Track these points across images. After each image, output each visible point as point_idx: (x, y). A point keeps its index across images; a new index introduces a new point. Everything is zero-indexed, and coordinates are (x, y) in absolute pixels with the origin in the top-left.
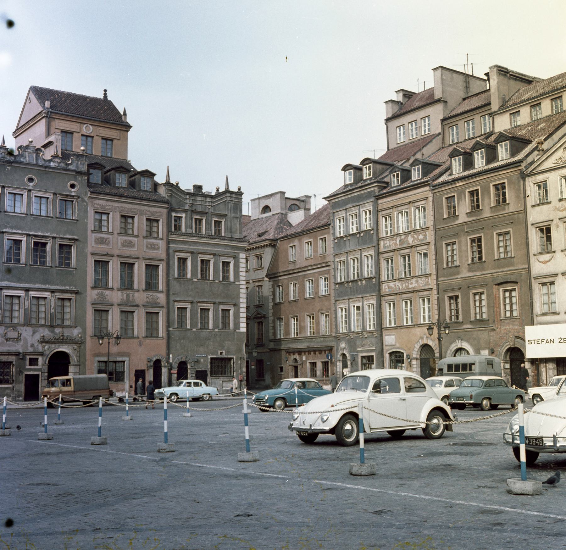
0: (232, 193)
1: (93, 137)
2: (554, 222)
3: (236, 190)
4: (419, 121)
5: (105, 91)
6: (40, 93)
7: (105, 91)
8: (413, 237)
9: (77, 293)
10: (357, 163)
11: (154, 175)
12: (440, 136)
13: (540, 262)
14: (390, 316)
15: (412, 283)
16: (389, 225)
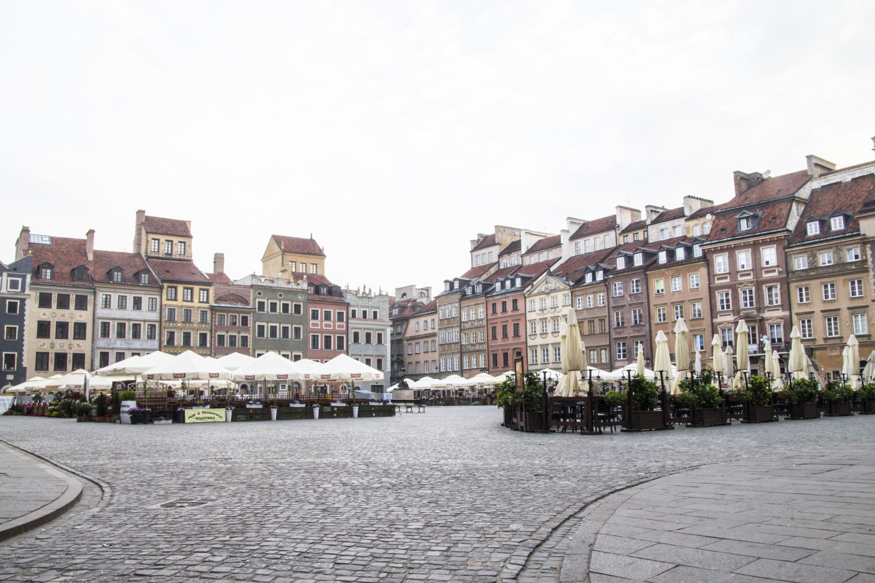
6: (277, 239)
10: (451, 279)
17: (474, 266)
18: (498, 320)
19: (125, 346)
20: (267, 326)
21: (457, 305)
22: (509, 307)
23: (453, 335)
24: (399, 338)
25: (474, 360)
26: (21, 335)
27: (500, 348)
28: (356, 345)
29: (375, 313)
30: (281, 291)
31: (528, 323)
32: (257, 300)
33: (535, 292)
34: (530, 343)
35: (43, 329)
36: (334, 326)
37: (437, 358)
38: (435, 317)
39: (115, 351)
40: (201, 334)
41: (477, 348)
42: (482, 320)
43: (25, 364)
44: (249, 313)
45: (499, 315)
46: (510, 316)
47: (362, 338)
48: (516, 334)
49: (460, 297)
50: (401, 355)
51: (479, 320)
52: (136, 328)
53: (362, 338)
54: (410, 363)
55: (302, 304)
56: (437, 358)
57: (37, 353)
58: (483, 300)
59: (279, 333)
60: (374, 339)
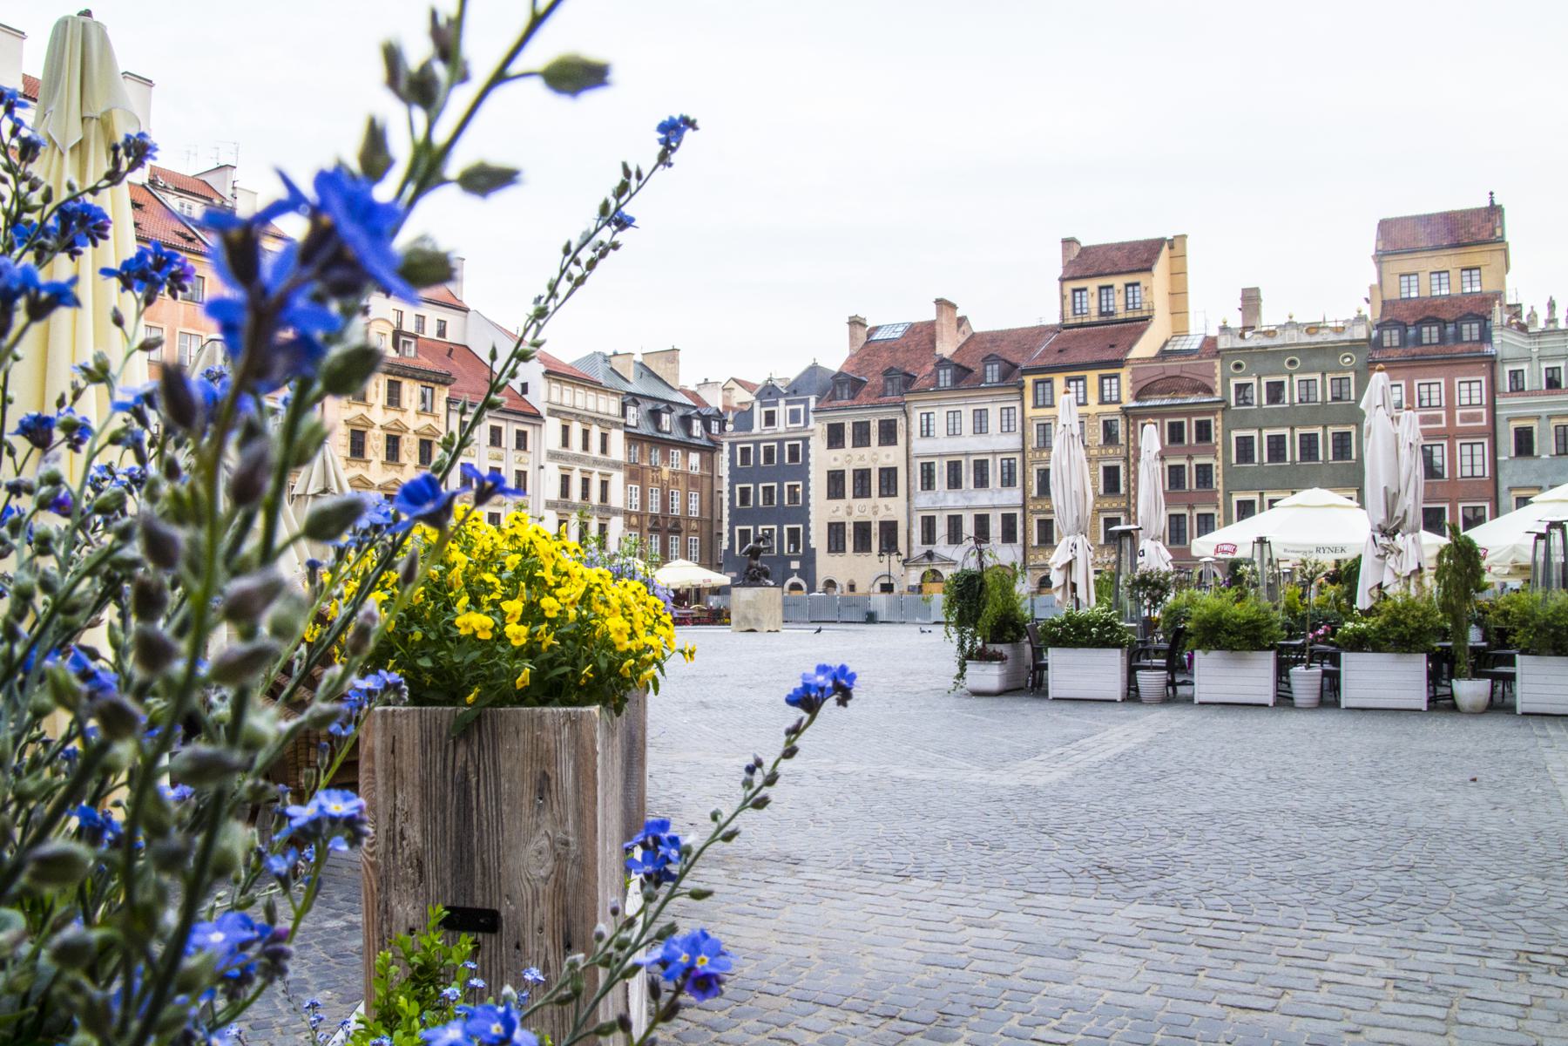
6: (1385, 226)
19: (962, 503)
20: (1260, 438)
26: (806, 497)
28: (1523, 462)
30: (1293, 352)
32: (1233, 382)
35: (835, 482)
36: (1451, 418)
39: (946, 514)
40: (1106, 469)
43: (813, 543)
44: (1213, 412)
52: (981, 468)
55: (1352, 375)
57: (830, 525)
59: (1293, 452)
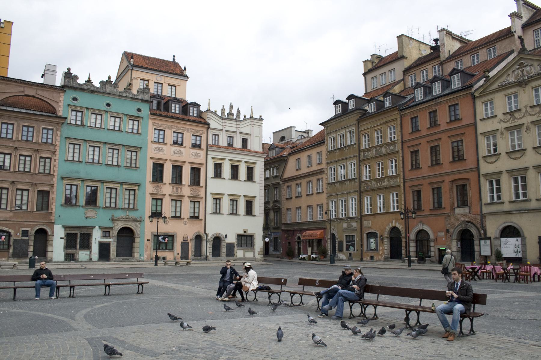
0: (255, 119)
1: (162, 84)
2: (500, 131)
3: (258, 117)
4: (387, 73)
5: (174, 56)
7: (174, 56)
8: (386, 148)
9: (139, 185)
11: (200, 106)
12: (402, 82)
13: (488, 163)
14: (368, 206)
15: (384, 182)
16: (367, 141)
17: (368, 92)
18: (421, 141)
21: (354, 128)
22: (443, 117)
23: (347, 171)
24: (277, 181)
25: (380, 202)
27: (425, 182)
29: (245, 142)
31: (481, 139)
33: (495, 86)
34: (485, 168)
37: (324, 202)
38: (323, 149)
41: (386, 183)
42: (393, 143)
45: (424, 133)
46: (444, 131)
47: (226, 171)
48: (458, 157)
49: (358, 117)
50: (277, 201)
51: (388, 144)
53: (226, 171)
54: (289, 209)
56: (324, 202)
58: (396, 115)
60: (243, 173)
